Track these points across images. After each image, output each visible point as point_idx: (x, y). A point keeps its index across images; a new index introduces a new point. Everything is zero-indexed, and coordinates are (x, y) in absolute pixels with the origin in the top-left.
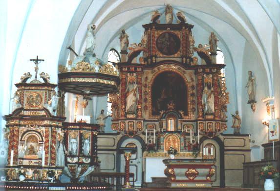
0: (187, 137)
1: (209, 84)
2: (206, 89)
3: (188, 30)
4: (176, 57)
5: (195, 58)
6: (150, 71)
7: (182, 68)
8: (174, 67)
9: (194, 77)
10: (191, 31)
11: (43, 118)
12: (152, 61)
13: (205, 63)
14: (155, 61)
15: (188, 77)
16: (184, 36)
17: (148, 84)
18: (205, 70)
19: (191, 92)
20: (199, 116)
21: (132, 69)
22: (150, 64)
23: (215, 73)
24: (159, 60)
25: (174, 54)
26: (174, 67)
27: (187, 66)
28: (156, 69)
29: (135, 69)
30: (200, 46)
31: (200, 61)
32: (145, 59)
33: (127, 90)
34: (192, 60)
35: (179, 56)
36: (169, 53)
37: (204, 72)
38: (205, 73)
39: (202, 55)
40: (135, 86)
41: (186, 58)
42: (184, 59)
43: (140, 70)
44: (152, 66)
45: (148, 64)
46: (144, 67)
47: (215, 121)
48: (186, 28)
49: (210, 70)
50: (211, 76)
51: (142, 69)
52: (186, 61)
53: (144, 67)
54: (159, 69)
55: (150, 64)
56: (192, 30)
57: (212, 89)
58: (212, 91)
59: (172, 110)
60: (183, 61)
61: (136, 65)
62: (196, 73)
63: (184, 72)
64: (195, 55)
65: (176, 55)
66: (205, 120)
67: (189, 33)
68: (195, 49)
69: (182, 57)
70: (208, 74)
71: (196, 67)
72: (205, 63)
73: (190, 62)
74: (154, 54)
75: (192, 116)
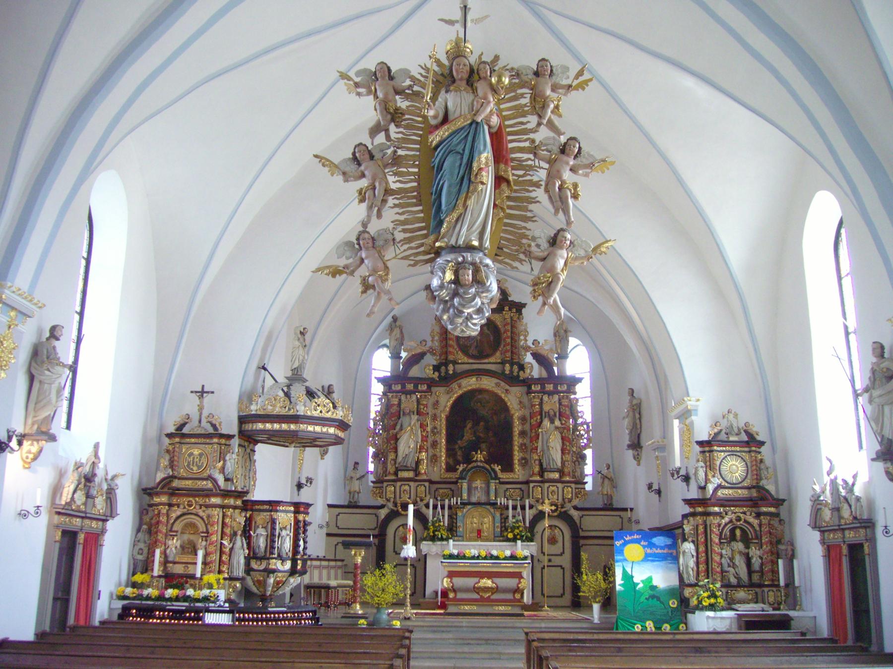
0: (505, 512)
1: (552, 413)
2: (546, 423)
3: (517, 311)
4: (491, 363)
5: (529, 363)
6: (442, 389)
7: (503, 384)
8: (488, 383)
9: (525, 399)
10: (521, 314)
11: (207, 493)
12: (447, 370)
13: (545, 374)
14: (454, 370)
15: (513, 398)
16: (507, 324)
17: (438, 415)
18: (544, 387)
19: (520, 428)
20: (533, 474)
21: (410, 387)
22: (444, 377)
23: (563, 392)
24: (460, 368)
25: (488, 356)
26: (488, 383)
27: (513, 380)
28: (455, 386)
29: (416, 386)
30: (535, 342)
31: (536, 371)
32: (436, 368)
33: (398, 427)
34: (522, 368)
35: (499, 361)
36: (481, 355)
37: (543, 391)
38: (545, 393)
39: (541, 359)
40: (415, 417)
41: (512, 364)
42: (507, 367)
43: (425, 387)
44: (446, 380)
45: (440, 376)
46: (431, 383)
47: (563, 482)
48: (510, 309)
49: (555, 387)
50: (556, 397)
51: (429, 387)
52: (511, 371)
53: (431, 383)
54: (460, 386)
55: (444, 377)
56: (524, 310)
57: (557, 423)
58: (557, 428)
59: (479, 464)
60: (504, 370)
61: (418, 381)
62: (529, 392)
63: (507, 390)
64: (529, 358)
65: (492, 360)
66: (542, 482)
67: (518, 318)
68: (527, 349)
69: (503, 363)
70: (550, 394)
71: (527, 383)
72: (545, 374)
73: (518, 373)
74: (451, 357)
75: (519, 473)
